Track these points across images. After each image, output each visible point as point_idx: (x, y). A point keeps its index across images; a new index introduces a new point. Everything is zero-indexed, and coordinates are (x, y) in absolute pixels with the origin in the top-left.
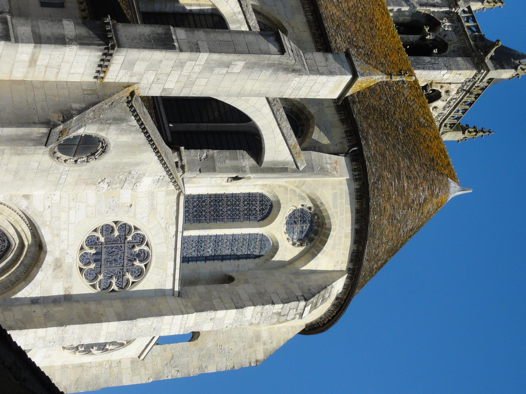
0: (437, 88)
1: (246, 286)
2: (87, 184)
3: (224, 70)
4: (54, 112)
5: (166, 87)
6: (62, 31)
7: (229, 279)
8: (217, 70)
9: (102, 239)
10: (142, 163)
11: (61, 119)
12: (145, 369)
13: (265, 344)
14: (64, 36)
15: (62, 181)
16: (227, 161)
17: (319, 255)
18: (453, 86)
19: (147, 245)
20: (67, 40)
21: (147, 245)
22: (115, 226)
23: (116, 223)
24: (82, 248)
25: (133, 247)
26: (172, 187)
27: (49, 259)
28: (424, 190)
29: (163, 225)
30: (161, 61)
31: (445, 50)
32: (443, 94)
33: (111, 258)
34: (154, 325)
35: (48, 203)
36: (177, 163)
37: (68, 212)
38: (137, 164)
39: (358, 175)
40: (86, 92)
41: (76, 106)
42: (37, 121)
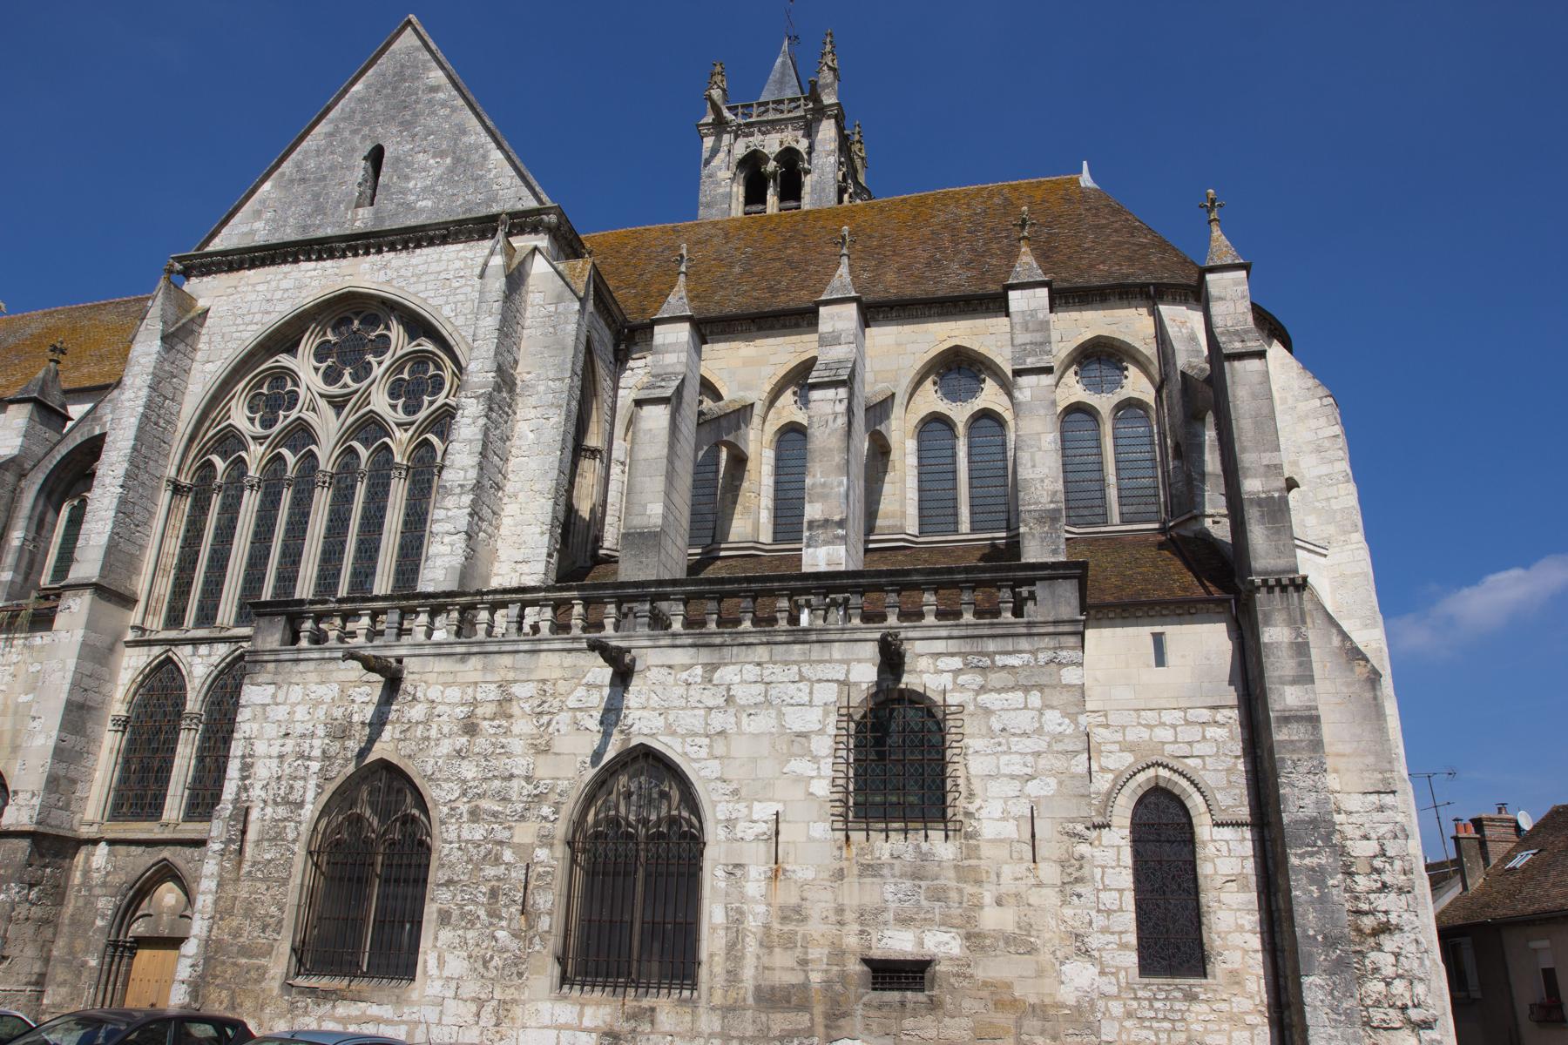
1: (1302, 465)
4: (1352, 670)
11: (1362, 663)
20: (1300, 640)
31: (797, 152)
36: (1214, 522)
41: (1336, 641)
42: (1371, 695)
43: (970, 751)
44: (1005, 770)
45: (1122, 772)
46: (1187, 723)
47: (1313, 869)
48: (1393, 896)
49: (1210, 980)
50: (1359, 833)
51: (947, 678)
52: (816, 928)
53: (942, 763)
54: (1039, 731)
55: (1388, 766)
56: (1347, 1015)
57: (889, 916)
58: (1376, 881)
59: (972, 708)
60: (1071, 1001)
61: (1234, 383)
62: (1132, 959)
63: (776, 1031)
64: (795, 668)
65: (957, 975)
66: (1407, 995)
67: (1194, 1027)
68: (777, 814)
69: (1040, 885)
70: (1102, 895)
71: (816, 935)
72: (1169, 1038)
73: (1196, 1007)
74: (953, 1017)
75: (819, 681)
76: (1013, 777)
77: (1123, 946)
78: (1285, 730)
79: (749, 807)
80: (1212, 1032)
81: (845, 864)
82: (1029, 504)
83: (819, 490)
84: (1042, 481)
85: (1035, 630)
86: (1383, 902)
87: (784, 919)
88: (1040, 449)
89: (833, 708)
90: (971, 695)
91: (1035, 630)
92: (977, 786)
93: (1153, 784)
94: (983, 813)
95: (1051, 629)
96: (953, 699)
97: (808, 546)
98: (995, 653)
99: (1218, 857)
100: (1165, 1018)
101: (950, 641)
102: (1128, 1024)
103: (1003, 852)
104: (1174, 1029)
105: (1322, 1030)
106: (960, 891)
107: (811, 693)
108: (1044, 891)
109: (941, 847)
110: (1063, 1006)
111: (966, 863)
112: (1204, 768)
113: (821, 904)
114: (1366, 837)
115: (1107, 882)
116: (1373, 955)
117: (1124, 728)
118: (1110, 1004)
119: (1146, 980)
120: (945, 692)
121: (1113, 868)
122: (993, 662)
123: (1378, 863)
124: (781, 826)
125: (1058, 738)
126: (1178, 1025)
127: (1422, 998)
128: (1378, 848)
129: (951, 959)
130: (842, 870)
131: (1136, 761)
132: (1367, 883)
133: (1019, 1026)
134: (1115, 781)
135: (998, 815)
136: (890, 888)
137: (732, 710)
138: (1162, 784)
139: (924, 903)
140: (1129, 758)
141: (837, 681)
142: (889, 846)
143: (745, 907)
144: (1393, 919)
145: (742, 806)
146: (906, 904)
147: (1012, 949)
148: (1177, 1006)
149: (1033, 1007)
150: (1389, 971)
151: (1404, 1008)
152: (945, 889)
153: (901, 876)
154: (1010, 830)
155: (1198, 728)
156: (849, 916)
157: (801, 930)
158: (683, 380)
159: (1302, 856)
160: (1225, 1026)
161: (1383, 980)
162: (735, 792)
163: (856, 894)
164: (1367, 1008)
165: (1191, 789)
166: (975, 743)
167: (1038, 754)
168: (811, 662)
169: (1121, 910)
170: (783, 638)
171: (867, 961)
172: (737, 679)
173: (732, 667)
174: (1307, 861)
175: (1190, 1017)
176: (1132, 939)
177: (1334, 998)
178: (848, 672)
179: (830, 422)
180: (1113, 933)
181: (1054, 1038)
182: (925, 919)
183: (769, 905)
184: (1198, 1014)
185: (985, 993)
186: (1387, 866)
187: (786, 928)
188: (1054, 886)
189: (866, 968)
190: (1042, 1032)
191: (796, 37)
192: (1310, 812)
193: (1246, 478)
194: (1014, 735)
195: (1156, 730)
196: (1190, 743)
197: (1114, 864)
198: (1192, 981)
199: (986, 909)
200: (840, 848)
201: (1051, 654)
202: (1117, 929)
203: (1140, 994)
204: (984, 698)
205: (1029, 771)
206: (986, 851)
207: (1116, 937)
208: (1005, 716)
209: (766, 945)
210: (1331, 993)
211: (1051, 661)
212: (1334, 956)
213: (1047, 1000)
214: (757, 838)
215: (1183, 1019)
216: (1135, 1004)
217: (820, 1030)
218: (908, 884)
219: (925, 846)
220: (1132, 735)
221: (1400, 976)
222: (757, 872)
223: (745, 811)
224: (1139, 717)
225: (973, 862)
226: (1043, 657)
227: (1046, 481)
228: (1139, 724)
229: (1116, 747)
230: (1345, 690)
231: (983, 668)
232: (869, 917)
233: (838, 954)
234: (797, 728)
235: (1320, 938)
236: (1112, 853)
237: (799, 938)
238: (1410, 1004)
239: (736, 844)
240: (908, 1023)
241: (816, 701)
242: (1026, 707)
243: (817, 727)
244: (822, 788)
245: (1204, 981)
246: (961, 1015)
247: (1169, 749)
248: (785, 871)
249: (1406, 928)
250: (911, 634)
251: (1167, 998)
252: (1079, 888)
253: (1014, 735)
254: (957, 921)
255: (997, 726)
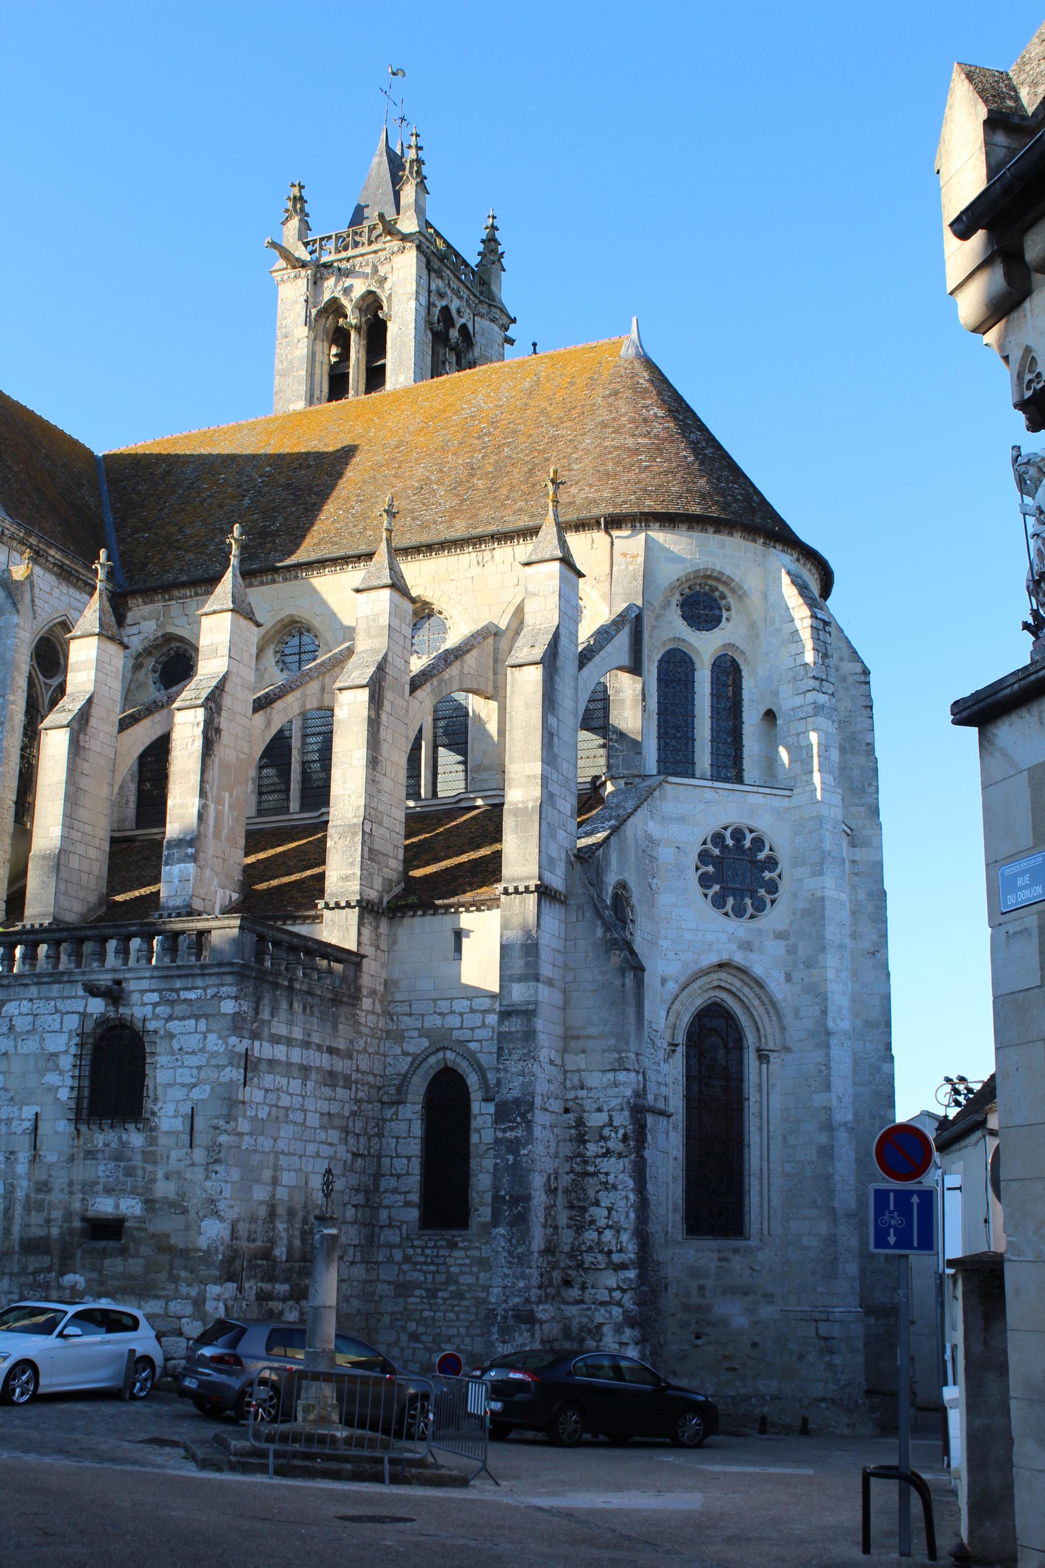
0: (436, 311)
1: (781, 695)
2: (653, 906)
3: (556, 739)
5: (569, 814)
6: (517, 947)
7: (770, 715)
8: (556, 750)
9: (716, 888)
10: (635, 836)
11: (617, 952)
12: (864, 828)
13: (842, 659)
14: (523, 944)
15: (648, 937)
16: (626, 714)
17: (745, 588)
18: (433, 287)
19: (725, 828)
21: (725, 828)
22: (700, 872)
23: (697, 869)
24: (726, 914)
25: (727, 846)
26: (656, 794)
27: (739, 958)
28: (646, 407)
29: (702, 806)
30: (548, 823)
32: (444, 303)
33: (740, 877)
34: (831, 829)
35: (672, 955)
36: (626, 784)
37: (684, 930)
38: (636, 843)
39: (640, 522)
40: (580, 918)
41: (599, 932)
43: (159, 1065)
44: (179, 1080)
45: (418, 1055)
46: (473, 1011)
47: (511, 1141)
48: (613, 1160)
49: (469, 1232)
50: (595, 1106)
51: (149, 1009)
52: (57, 1196)
53: (143, 1075)
54: (202, 1050)
55: (625, 1046)
56: (518, 1258)
57: (100, 1187)
58: (602, 1147)
59: (162, 1032)
60: (205, 1247)
61: (512, 693)
62: (414, 1214)
63: (31, 1269)
64: (53, 1003)
65: (138, 1229)
66: (614, 1242)
67: (453, 1269)
68: (37, 1114)
69: (193, 1165)
70: (395, 1161)
71: (56, 1202)
72: (434, 1278)
73: (457, 1254)
74: (133, 1258)
75: (67, 1013)
76: (183, 1085)
77: (408, 1204)
78: (507, 1023)
79: (20, 1109)
80: (465, 1273)
81: (75, 1150)
82: (338, 819)
83: (177, 811)
84: (350, 796)
85: (207, 971)
86: (606, 1165)
87: (38, 1190)
88: (351, 766)
89: (74, 1034)
90: (162, 1022)
91: (207, 971)
92: (160, 1092)
93: (442, 1066)
94: (162, 1113)
95: (216, 970)
96: (151, 1026)
97: (166, 864)
98: (180, 989)
99: (484, 1128)
100: (432, 1263)
101: (153, 981)
102: (405, 1267)
103: (171, 1141)
104: (437, 1272)
105: (500, 1270)
106: (144, 1169)
107: (62, 1022)
108: (196, 1169)
109: (136, 1139)
110: (200, 1250)
111: (149, 1149)
112: (481, 1052)
113: (59, 1180)
114: (599, 1110)
115: (399, 1150)
116: (592, 1210)
117: (423, 1015)
118: (394, 1251)
119: (421, 1232)
120: (144, 1020)
121: (405, 1138)
122: (179, 996)
123: (606, 1132)
124: (40, 1124)
125: (214, 1055)
126: (442, 1267)
127: (624, 1244)
128: (607, 1118)
129: (135, 1217)
130: (73, 1155)
131: (430, 1045)
132: (595, 1149)
133: (171, 1264)
134: (412, 1063)
135: (171, 1113)
136: (102, 1168)
137: (12, 1036)
138: (450, 1065)
139: (122, 1178)
140: (424, 1042)
141: (78, 1013)
142: (102, 1138)
143: (15, 1182)
144: (611, 1179)
145: (15, 1109)
146: (111, 1179)
147: (173, 1210)
148: (442, 1252)
149: (181, 1250)
150: (602, 1223)
151: (610, 1252)
152: (134, 1168)
153: (109, 1159)
154: (179, 1124)
155: (479, 1015)
156: (77, 1188)
157: (48, 1198)
158: (90, 701)
159: (504, 1131)
160: (475, 1269)
161: (597, 1230)
162: (12, 1099)
163: (84, 1172)
164: (582, 1252)
165: (469, 1070)
166: (162, 1060)
167: (199, 1068)
168: (63, 998)
169: (407, 1174)
170: (46, 980)
171: (84, 1219)
172: (16, 1012)
173: (15, 1003)
174: (508, 1134)
175: (449, 1260)
176: (415, 1198)
177: (511, 1245)
178: (86, 1005)
179: (189, 746)
180: (400, 1193)
181: (192, 1272)
182: (121, 1190)
183: (29, 1180)
184: (456, 1259)
185: (153, 1242)
186: (613, 1134)
187: (40, 1196)
188: (202, 1165)
189: (85, 1225)
190: (185, 1268)
191: (403, 119)
192: (516, 1093)
193: (510, 787)
194: (187, 1053)
195: (447, 1017)
196: (472, 1029)
197: (405, 1135)
198: (454, 1232)
199: (158, 1183)
200: (73, 1139)
201: (215, 990)
202: (404, 1190)
203: (416, 1243)
204: (174, 1026)
205: (194, 1080)
206: (162, 1140)
207: (403, 1196)
208: (182, 1038)
209: (27, 1209)
210: (510, 1241)
211: (216, 995)
212: (516, 1212)
213: (190, 1246)
214: (24, 1132)
215: (445, 1263)
216: (411, 1251)
217: (56, 1267)
218: (112, 1165)
219: (125, 1137)
220: (427, 1025)
221: (608, 1227)
222: (24, 1156)
223: (17, 1113)
224: (435, 1006)
225: (153, 1148)
226: (210, 992)
227: (353, 797)
228: (435, 1012)
229: (415, 1033)
230: (600, 978)
231: (173, 1001)
232: (89, 1188)
233: (68, 1216)
234: (52, 1049)
235: (507, 1198)
236: (404, 1126)
237: (46, 1203)
238: (614, 1249)
239: (12, 1137)
240: (107, 1262)
241: (65, 1029)
242: (196, 1032)
243: (63, 1048)
244: (64, 1094)
245: (463, 1232)
246: (138, 1256)
247: (456, 1034)
248: (40, 1156)
249: (620, 1187)
250: (128, 975)
251: (435, 1247)
252: (217, 1167)
253: (187, 1053)
254: (140, 1191)
255: (176, 1047)
